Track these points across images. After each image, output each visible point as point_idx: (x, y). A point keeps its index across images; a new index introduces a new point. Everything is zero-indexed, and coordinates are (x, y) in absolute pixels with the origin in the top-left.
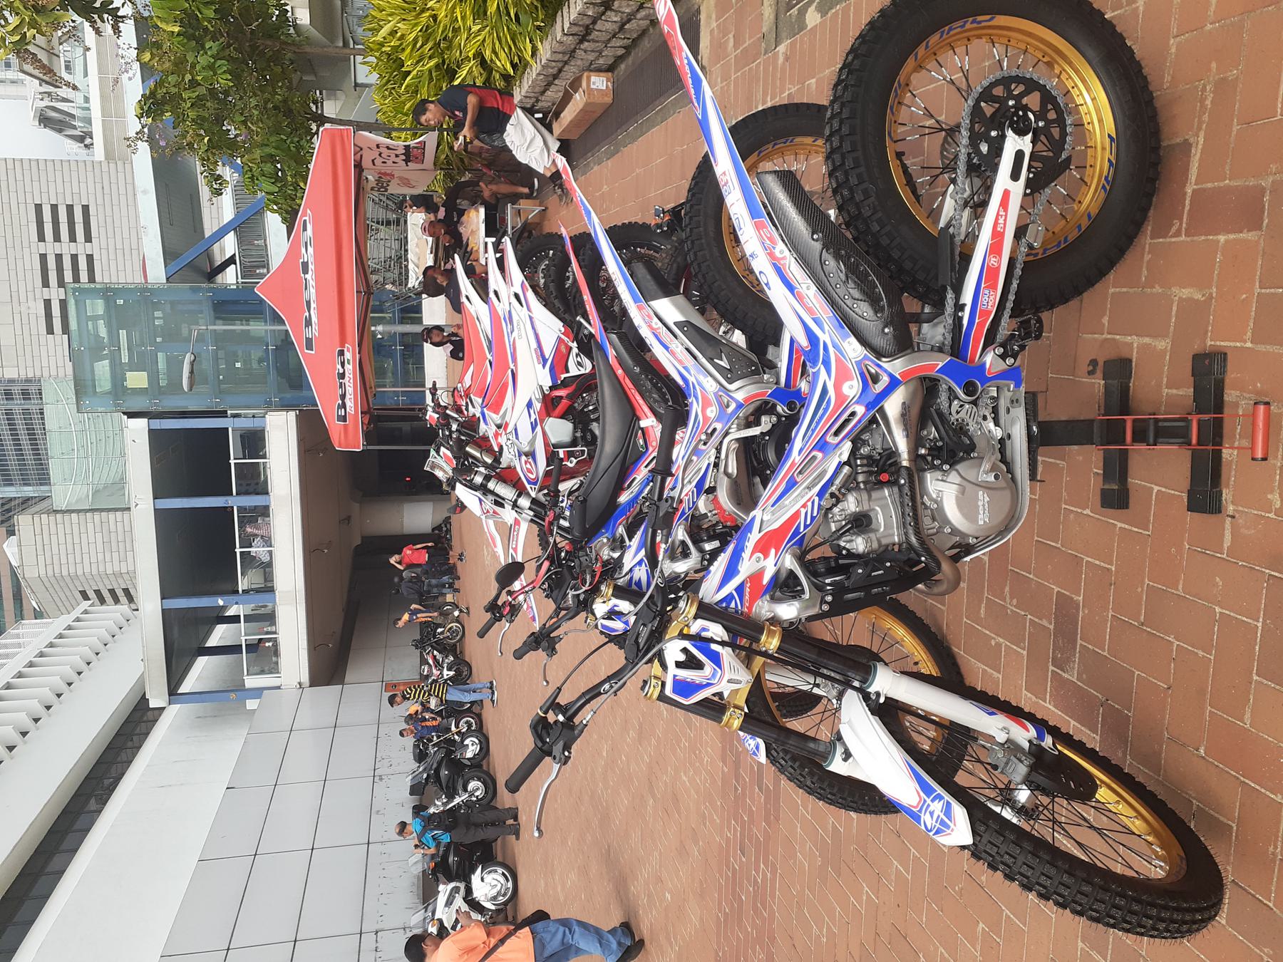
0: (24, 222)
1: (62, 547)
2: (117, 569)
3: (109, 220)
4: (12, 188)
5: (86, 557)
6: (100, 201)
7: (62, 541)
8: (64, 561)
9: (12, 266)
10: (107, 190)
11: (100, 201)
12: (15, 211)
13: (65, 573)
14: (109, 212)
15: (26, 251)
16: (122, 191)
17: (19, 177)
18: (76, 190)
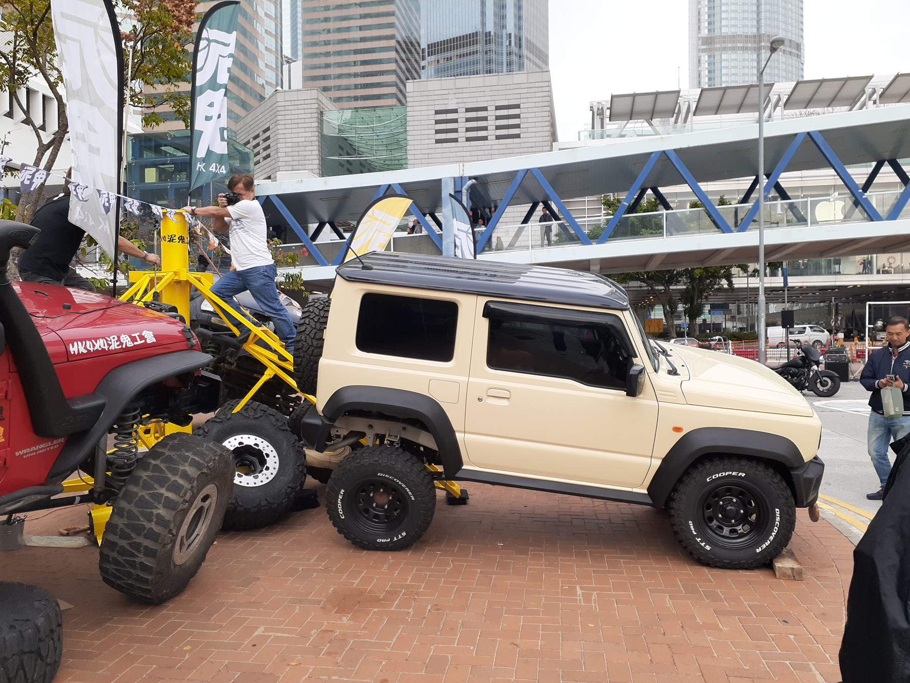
0: (508, 97)
1: (296, 117)
2: (281, 150)
4: (530, 90)
5: (289, 131)
6: (523, 145)
7: (300, 116)
8: (287, 117)
9: (479, 89)
11: (523, 145)
15: (489, 99)
18: (530, 130)
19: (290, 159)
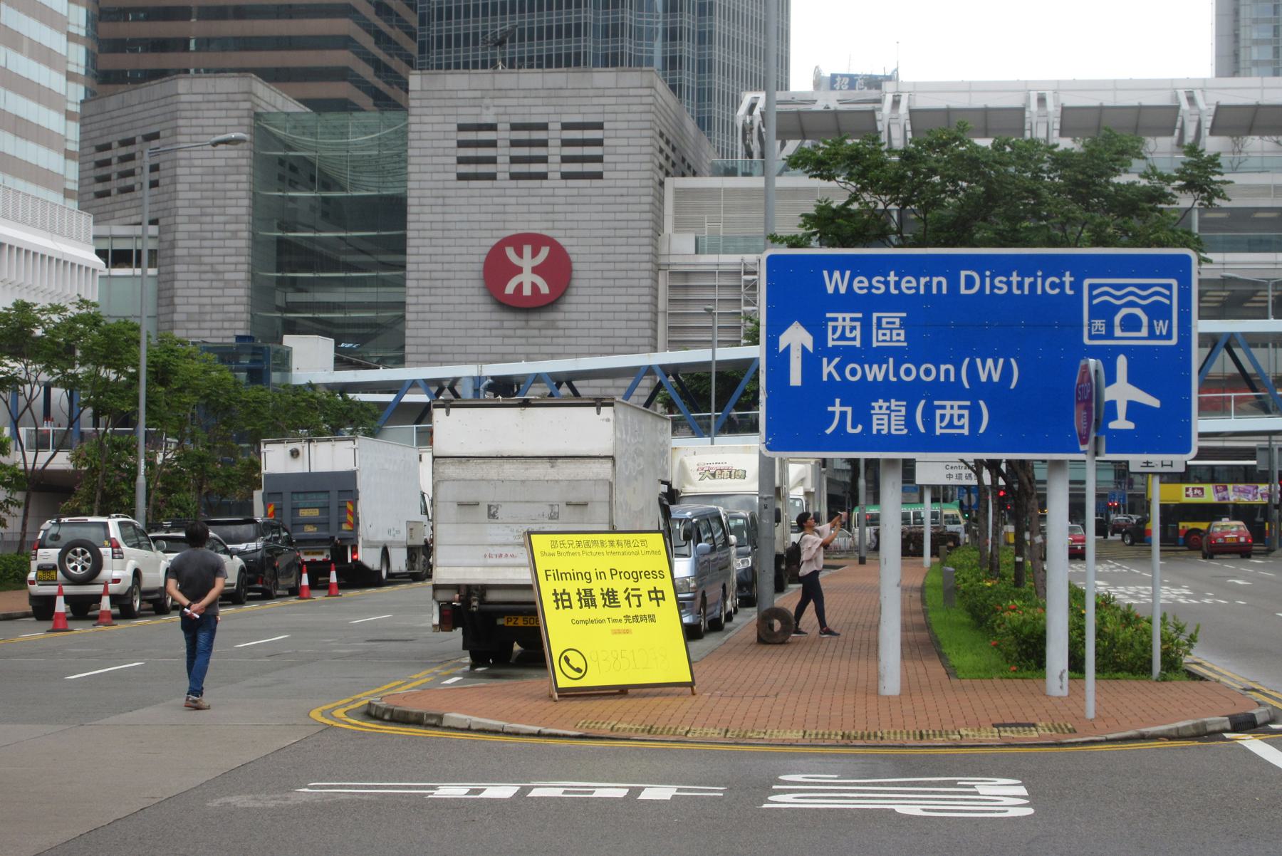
0: (583, 109)
2: (181, 179)
3: (586, 200)
6: (607, 191)
10: (619, 200)
12: (595, 101)
13: (181, 122)
14: (595, 200)
16: (619, 216)
17: (634, 108)
18: (619, 167)
19: (198, 195)
